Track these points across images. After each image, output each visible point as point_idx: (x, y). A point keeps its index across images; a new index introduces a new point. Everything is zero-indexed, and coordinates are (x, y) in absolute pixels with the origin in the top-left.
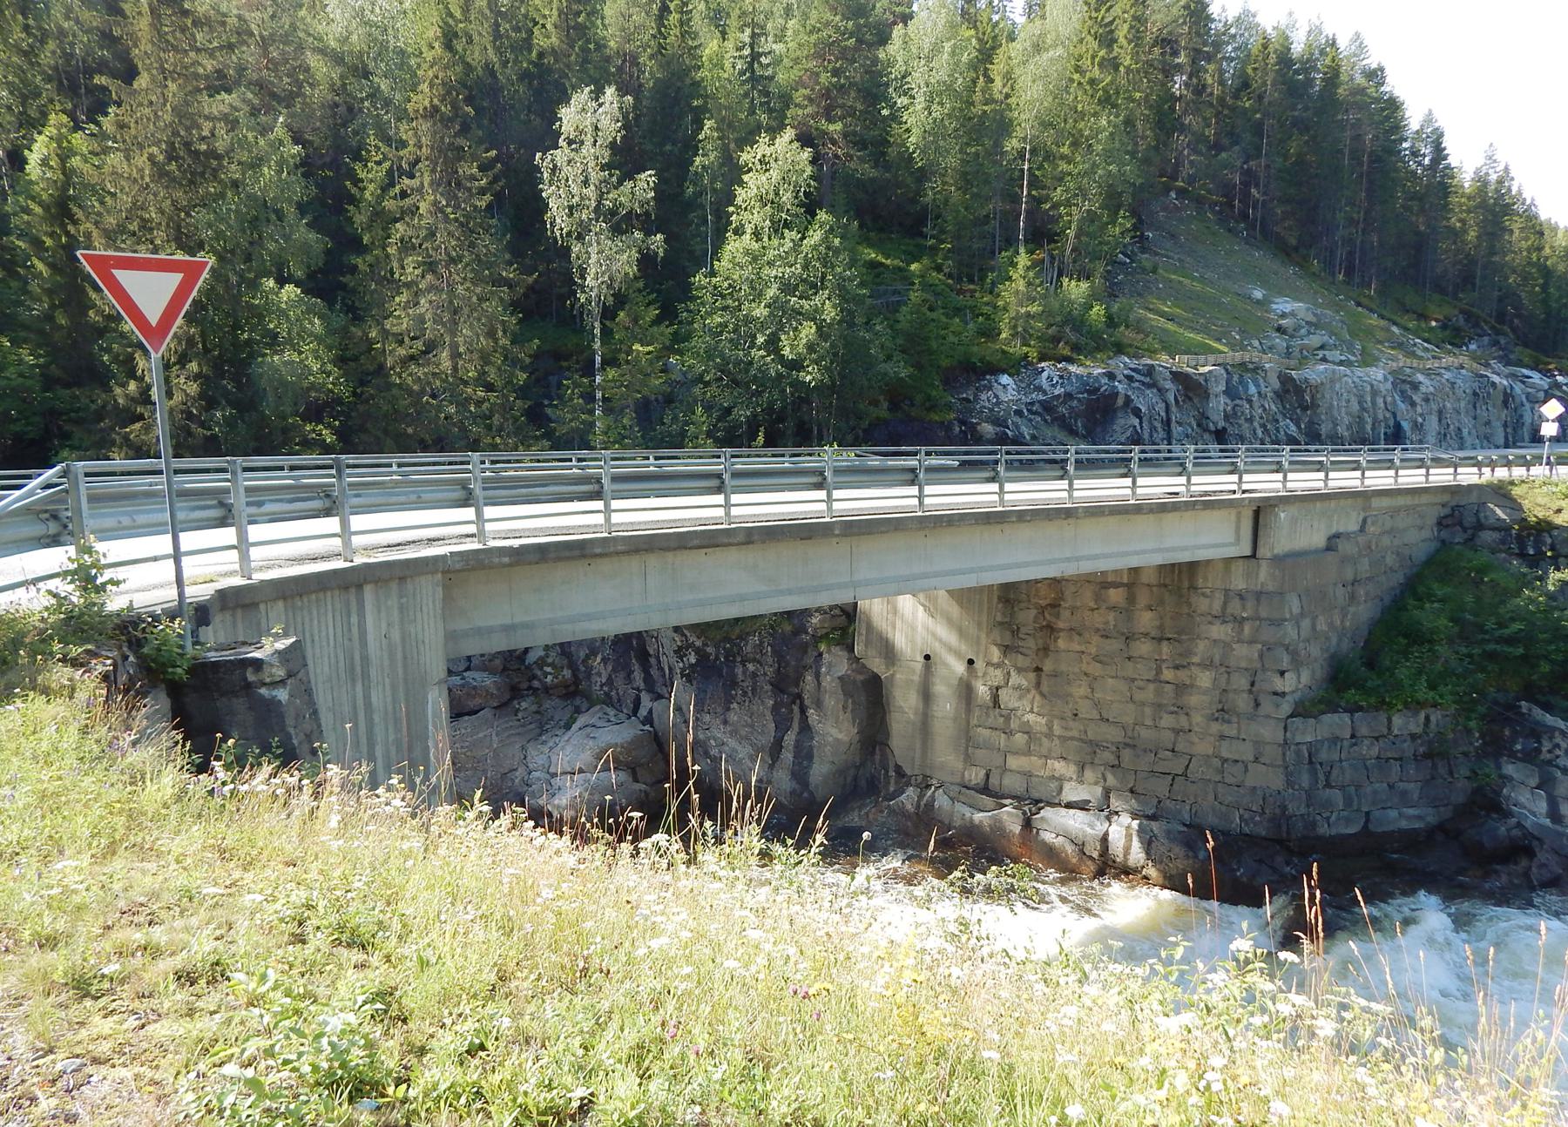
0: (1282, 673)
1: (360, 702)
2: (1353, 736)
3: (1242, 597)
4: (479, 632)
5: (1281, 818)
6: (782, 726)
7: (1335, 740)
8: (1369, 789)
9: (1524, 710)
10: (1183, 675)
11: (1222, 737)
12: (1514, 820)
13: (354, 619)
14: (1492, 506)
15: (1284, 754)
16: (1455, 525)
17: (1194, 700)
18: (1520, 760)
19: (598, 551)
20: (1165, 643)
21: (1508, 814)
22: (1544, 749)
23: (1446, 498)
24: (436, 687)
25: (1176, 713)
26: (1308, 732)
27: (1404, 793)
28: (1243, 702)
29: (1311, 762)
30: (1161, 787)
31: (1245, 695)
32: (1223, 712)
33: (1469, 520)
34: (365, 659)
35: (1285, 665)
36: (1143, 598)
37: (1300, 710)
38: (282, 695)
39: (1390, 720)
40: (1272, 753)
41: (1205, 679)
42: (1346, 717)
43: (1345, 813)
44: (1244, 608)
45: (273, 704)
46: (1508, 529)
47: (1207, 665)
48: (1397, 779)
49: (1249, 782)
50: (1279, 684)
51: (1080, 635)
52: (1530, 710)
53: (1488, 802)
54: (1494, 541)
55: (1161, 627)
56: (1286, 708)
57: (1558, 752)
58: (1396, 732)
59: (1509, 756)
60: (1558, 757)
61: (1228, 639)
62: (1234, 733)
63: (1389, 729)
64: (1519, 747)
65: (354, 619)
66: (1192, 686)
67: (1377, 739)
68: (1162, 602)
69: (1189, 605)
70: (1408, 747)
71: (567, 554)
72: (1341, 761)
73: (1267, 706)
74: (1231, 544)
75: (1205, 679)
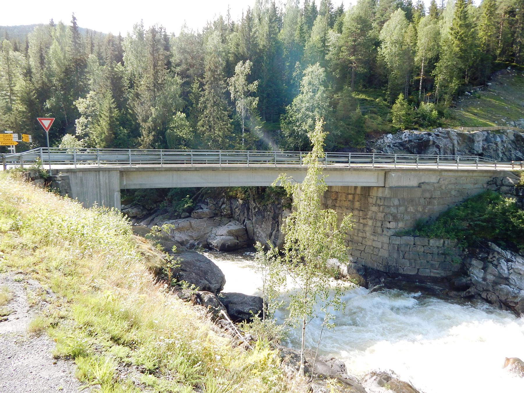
0: (389, 222)
1: (98, 192)
2: (414, 244)
3: (380, 199)
4: (134, 184)
5: (387, 266)
6: (273, 229)
7: (407, 245)
8: (419, 262)
9: (490, 245)
10: (365, 221)
11: (374, 240)
12: (470, 278)
13: (98, 177)
14: (508, 178)
15: (389, 247)
16: (493, 184)
17: (367, 229)
18: (479, 260)
19: (157, 169)
20: (361, 211)
21: (469, 276)
22: (489, 257)
23: (489, 174)
24: (117, 192)
25: (362, 232)
26: (398, 241)
27: (432, 265)
28: (379, 230)
29: (398, 250)
30: (357, 254)
31: (380, 228)
32: (374, 233)
33: (499, 182)
34: (100, 184)
35: (390, 220)
36: (357, 198)
37: (396, 234)
38: (60, 182)
39: (429, 241)
40: (386, 246)
41: (370, 223)
42: (412, 238)
43: (410, 268)
44: (381, 203)
45: (58, 183)
46: (512, 186)
47: (371, 219)
48: (431, 260)
49: (380, 255)
50: (388, 225)
51: (341, 208)
52: (491, 245)
53: (464, 271)
54: (507, 190)
55: (360, 207)
56: (390, 233)
57: (494, 259)
58: (431, 245)
59: (476, 258)
60: (494, 260)
61: (376, 211)
62: (376, 239)
63: (429, 244)
64: (480, 256)
65: (98, 177)
66: (367, 224)
67: (423, 246)
68: (361, 200)
69: (368, 200)
70: (435, 251)
71: (148, 170)
72: (409, 251)
73: (385, 232)
74: (376, 183)
75: (370, 223)
